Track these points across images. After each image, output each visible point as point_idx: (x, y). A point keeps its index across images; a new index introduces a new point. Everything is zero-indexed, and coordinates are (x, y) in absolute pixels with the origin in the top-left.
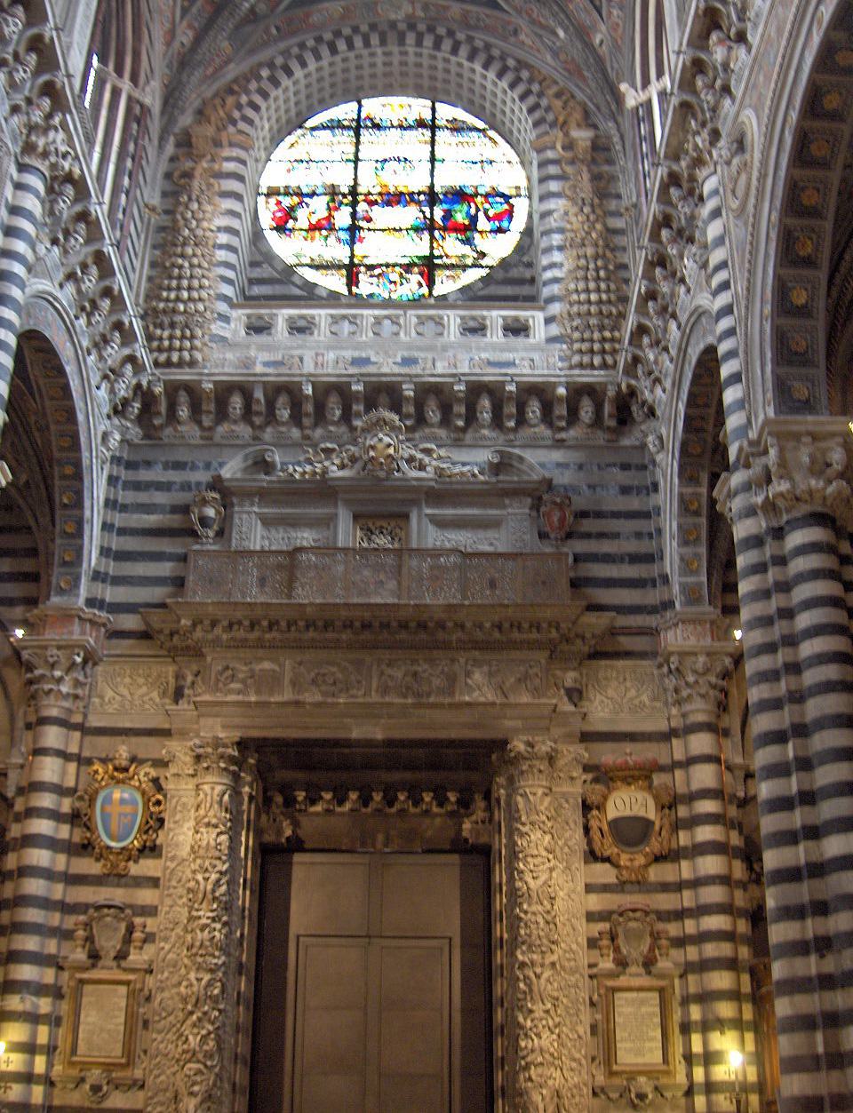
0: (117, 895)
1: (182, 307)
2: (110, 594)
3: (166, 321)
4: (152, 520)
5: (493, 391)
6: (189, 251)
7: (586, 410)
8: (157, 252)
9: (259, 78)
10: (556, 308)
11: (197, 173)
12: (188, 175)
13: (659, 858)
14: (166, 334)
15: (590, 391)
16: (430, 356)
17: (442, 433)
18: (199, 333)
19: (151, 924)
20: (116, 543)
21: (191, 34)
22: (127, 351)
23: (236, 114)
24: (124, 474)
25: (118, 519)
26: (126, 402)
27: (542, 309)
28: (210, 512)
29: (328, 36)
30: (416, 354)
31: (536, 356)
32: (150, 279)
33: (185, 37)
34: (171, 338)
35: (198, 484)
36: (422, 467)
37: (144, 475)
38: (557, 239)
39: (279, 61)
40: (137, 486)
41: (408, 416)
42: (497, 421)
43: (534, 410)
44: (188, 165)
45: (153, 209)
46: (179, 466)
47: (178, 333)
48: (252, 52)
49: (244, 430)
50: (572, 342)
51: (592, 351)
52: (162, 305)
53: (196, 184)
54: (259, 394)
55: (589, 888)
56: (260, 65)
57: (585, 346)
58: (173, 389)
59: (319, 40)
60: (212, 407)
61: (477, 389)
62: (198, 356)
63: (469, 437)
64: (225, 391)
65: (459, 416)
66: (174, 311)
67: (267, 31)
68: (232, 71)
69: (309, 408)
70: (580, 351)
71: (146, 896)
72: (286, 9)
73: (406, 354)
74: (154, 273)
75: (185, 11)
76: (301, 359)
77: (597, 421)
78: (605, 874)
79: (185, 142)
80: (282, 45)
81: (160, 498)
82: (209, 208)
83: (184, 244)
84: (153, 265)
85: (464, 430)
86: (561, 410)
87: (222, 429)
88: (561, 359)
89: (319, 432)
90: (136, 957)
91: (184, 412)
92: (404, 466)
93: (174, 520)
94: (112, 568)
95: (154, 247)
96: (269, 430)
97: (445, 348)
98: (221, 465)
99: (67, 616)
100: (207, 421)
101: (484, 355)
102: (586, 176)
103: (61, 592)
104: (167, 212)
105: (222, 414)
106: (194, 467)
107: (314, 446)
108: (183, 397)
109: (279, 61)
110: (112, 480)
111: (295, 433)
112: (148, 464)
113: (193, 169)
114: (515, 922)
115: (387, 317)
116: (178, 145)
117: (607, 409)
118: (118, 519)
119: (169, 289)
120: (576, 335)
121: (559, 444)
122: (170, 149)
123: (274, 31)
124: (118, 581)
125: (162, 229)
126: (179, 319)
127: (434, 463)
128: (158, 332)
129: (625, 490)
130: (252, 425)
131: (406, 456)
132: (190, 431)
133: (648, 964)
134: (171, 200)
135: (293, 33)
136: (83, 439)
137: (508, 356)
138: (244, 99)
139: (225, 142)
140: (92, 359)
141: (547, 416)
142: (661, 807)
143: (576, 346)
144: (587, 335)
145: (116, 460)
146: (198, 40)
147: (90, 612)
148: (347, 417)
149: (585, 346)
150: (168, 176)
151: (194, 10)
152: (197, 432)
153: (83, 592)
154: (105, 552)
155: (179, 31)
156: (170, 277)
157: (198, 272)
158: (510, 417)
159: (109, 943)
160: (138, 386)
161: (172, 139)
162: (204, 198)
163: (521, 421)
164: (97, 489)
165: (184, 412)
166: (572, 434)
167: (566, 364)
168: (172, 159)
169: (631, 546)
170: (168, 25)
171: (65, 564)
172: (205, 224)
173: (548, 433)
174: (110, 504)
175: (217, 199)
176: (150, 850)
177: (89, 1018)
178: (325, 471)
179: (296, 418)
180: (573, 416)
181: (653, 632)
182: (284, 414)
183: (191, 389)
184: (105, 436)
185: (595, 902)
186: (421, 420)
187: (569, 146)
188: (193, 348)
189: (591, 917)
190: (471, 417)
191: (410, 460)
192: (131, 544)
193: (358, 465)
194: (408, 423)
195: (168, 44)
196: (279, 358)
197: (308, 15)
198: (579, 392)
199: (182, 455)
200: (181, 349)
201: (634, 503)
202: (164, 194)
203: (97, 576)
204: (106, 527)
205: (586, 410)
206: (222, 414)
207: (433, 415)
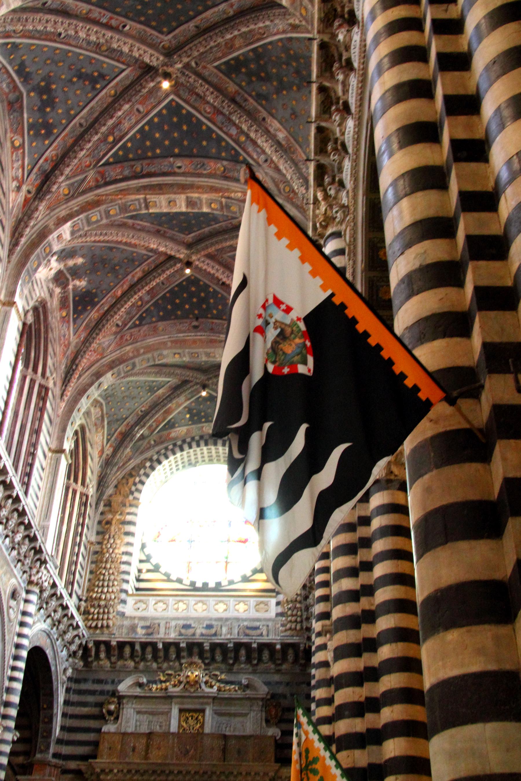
1: (103, 597)
2: (65, 750)
3: (96, 603)
4: (85, 710)
5: (247, 646)
6: (108, 566)
7: (291, 657)
8: (94, 566)
9: (145, 468)
11: (114, 522)
12: (109, 523)
14: (96, 611)
15: (294, 646)
16: (220, 623)
17: (223, 666)
18: (111, 610)
20: (69, 723)
21: (111, 449)
22: (75, 633)
23: (133, 488)
24: (74, 686)
25: (71, 710)
26: (75, 653)
27: (275, 597)
28: (112, 707)
29: (179, 443)
30: (214, 623)
31: (270, 624)
32: (89, 580)
33: (108, 451)
34: (98, 613)
35: (108, 692)
36: (211, 687)
37: (83, 686)
39: (155, 457)
40: (80, 692)
41: (207, 658)
42: (249, 660)
43: (266, 655)
44: (110, 516)
45: (92, 543)
46: (99, 681)
47: (101, 611)
48: (142, 453)
49: (131, 664)
50: (288, 616)
51: (296, 621)
52: (94, 595)
53: (113, 528)
54: (138, 647)
56: (146, 459)
57: (293, 619)
58: (97, 644)
59: (175, 445)
60: (116, 652)
61: (238, 646)
62: (111, 623)
63: (236, 667)
64: (121, 645)
65: (231, 658)
66: (100, 598)
67: (149, 443)
68: (132, 464)
69: (161, 654)
70: (291, 621)
72: (158, 432)
73: (208, 622)
74: (91, 577)
75: (108, 440)
76: (159, 625)
77: (296, 661)
79: (108, 504)
80: (157, 449)
81: (90, 699)
82: (118, 542)
83: (106, 562)
84: (91, 572)
85: (233, 664)
86: (279, 656)
87: (120, 663)
88: (282, 625)
89: (165, 665)
91: (103, 655)
92: (203, 686)
93: (95, 711)
94: (67, 736)
95: (92, 562)
96: (142, 664)
97: (227, 619)
98: (120, 682)
99: (45, 764)
100: (113, 659)
101: (245, 623)
103: (41, 752)
104: (99, 543)
105: (121, 656)
106: (106, 683)
107: (163, 672)
108: (103, 648)
109: (155, 457)
110: (68, 690)
111: (155, 665)
112: (85, 680)
113: (112, 519)
115: (200, 601)
116: (105, 505)
117: (301, 654)
118: (71, 710)
119: (98, 586)
120: (290, 612)
121: (278, 671)
122: (101, 508)
123: (152, 442)
124: (69, 743)
125: (96, 553)
126: (102, 603)
127: (218, 684)
128: (92, 610)
130: (134, 661)
131: (204, 680)
132: (106, 663)
134: (100, 537)
135: (162, 442)
136: (54, 678)
137: (257, 624)
138: (137, 479)
139: (127, 504)
140: (58, 643)
143: (289, 618)
144: (295, 612)
145: (70, 679)
146: (116, 451)
147: (54, 761)
148: (179, 657)
149: (293, 619)
150: (100, 523)
151: (113, 439)
152: (108, 664)
153: (52, 751)
154: (63, 728)
155: (106, 449)
156: (99, 580)
157: (112, 577)
158: (255, 659)
160: (81, 644)
161: (102, 504)
162: (116, 536)
163: (260, 660)
164: (61, 697)
165: (103, 655)
166: (284, 667)
167: (284, 629)
168: (102, 513)
170: (100, 448)
171: (43, 737)
172: (116, 551)
173: (273, 666)
174: (66, 703)
175: (123, 536)
178: (166, 689)
179: (155, 658)
180: (284, 659)
182: (150, 657)
183: (107, 644)
184: (65, 670)
186: (213, 659)
188: (108, 618)
190: (236, 659)
191: (206, 683)
193: (182, 686)
194: (207, 661)
195: (100, 457)
196: (148, 624)
197: (170, 433)
198: (286, 646)
199: (102, 676)
200: (103, 619)
202: (98, 533)
203: (59, 741)
204: (64, 715)
205: (291, 657)
206: (121, 656)
207: (219, 657)
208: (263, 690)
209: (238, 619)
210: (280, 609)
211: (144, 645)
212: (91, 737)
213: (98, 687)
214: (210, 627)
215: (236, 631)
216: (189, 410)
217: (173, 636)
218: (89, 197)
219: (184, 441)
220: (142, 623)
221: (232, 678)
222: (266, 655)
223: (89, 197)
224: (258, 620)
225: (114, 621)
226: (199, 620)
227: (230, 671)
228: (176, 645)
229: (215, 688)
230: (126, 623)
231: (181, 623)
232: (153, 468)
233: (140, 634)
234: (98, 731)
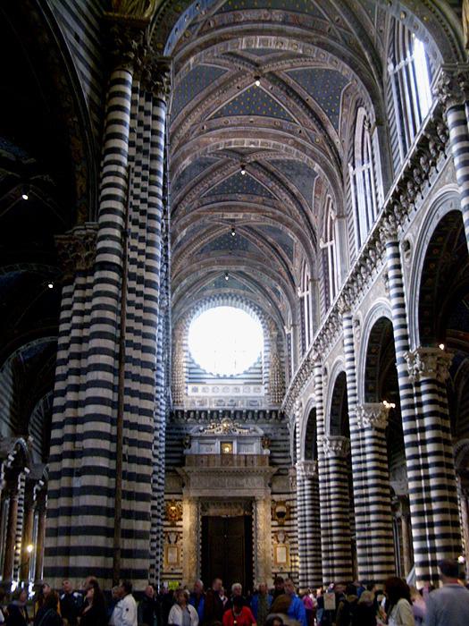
0: (174, 529)
7: (274, 416)
10: (266, 385)
13: (287, 520)
19: (181, 535)
28: (187, 441)
38: (268, 365)
43: (261, 416)
54: (197, 412)
55: (273, 526)
58: (177, 411)
64: (189, 412)
71: (179, 529)
78: (275, 523)
90: (178, 543)
93: (178, 443)
97: (240, 397)
102: (275, 345)
114: (257, 535)
121: (268, 423)
129: (282, 434)
133: (284, 542)
137: (255, 399)
141: (264, 417)
142: (287, 510)
148: (218, 417)
159: (173, 540)
163: (259, 417)
169: (284, 448)
176: (181, 520)
177: (170, 555)
180: (271, 417)
181: (287, 469)
183: (182, 412)
185: (274, 529)
187: (271, 336)
189: (272, 532)
192: (171, 449)
201: (284, 438)
205: (274, 416)
206: (189, 417)
208: (261, 432)
209: (246, 397)
210: (267, 391)
211: (201, 412)
212: (179, 455)
213: (177, 431)
214: (232, 401)
215: (245, 404)
216: (215, 282)
217: (214, 407)
218: (195, 212)
219: (211, 297)
220: (197, 399)
221: (245, 426)
222: (261, 416)
223: (195, 212)
224: (257, 397)
225: (184, 398)
226: (226, 398)
227: (244, 422)
228: (217, 412)
229: (238, 432)
230: (190, 399)
231: (217, 399)
232: (194, 313)
233: (197, 406)
234: (182, 452)
